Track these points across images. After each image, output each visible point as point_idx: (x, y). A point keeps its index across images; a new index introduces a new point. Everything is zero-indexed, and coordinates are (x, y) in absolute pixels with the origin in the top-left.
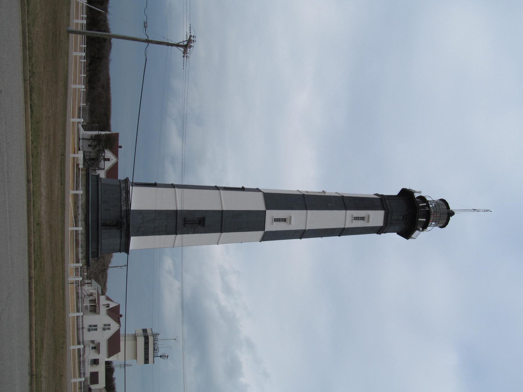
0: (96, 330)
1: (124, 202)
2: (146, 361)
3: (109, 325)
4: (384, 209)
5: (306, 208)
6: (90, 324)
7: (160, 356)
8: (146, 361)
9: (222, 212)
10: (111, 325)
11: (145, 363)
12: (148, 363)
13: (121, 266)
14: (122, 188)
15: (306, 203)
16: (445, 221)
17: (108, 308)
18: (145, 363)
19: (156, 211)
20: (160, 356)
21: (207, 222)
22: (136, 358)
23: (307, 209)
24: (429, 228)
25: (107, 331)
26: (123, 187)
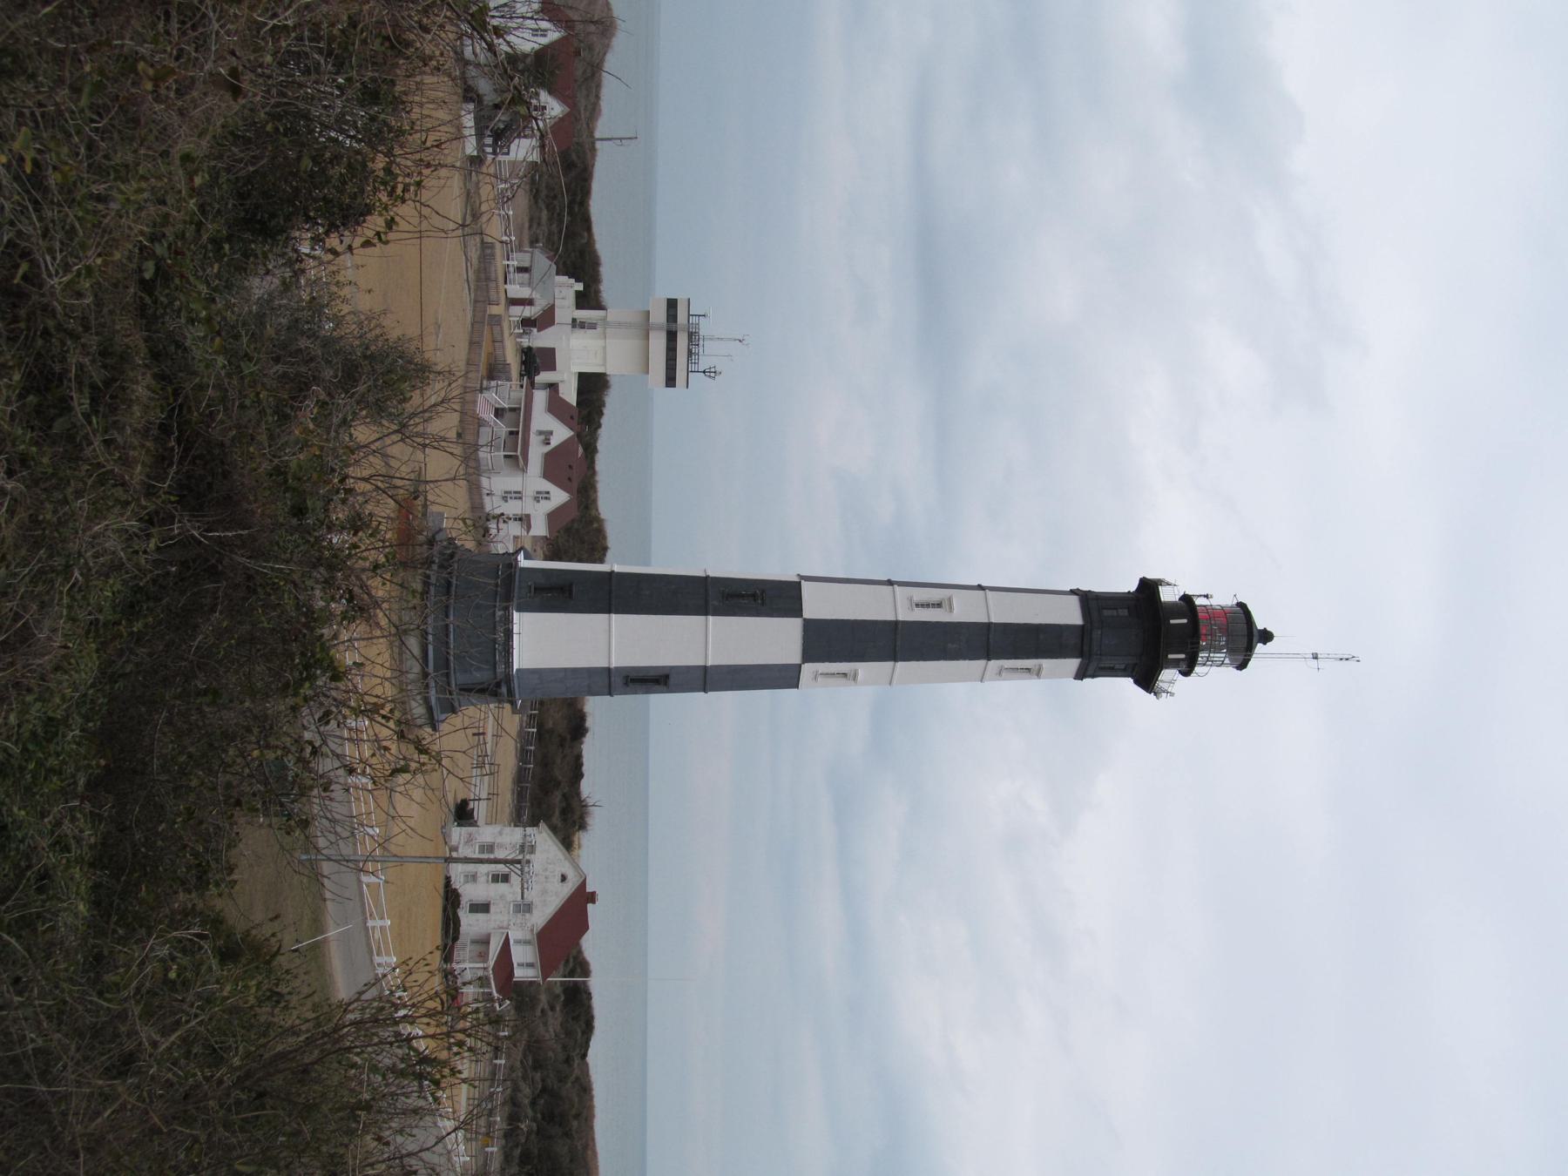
0: (521, 498)
1: (500, 653)
2: (671, 381)
3: (548, 493)
4: (1080, 654)
5: (894, 655)
6: (508, 489)
7: (704, 372)
8: (671, 381)
9: (705, 668)
10: (551, 493)
11: (668, 385)
12: (674, 386)
13: (621, 139)
14: (498, 619)
15: (898, 643)
16: (1245, 640)
17: (548, 448)
18: (668, 385)
19: (565, 670)
20: (704, 372)
21: (672, 681)
22: (648, 373)
23: (895, 659)
24: (1197, 669)
25: (542, 502)
26: (501, 617)
